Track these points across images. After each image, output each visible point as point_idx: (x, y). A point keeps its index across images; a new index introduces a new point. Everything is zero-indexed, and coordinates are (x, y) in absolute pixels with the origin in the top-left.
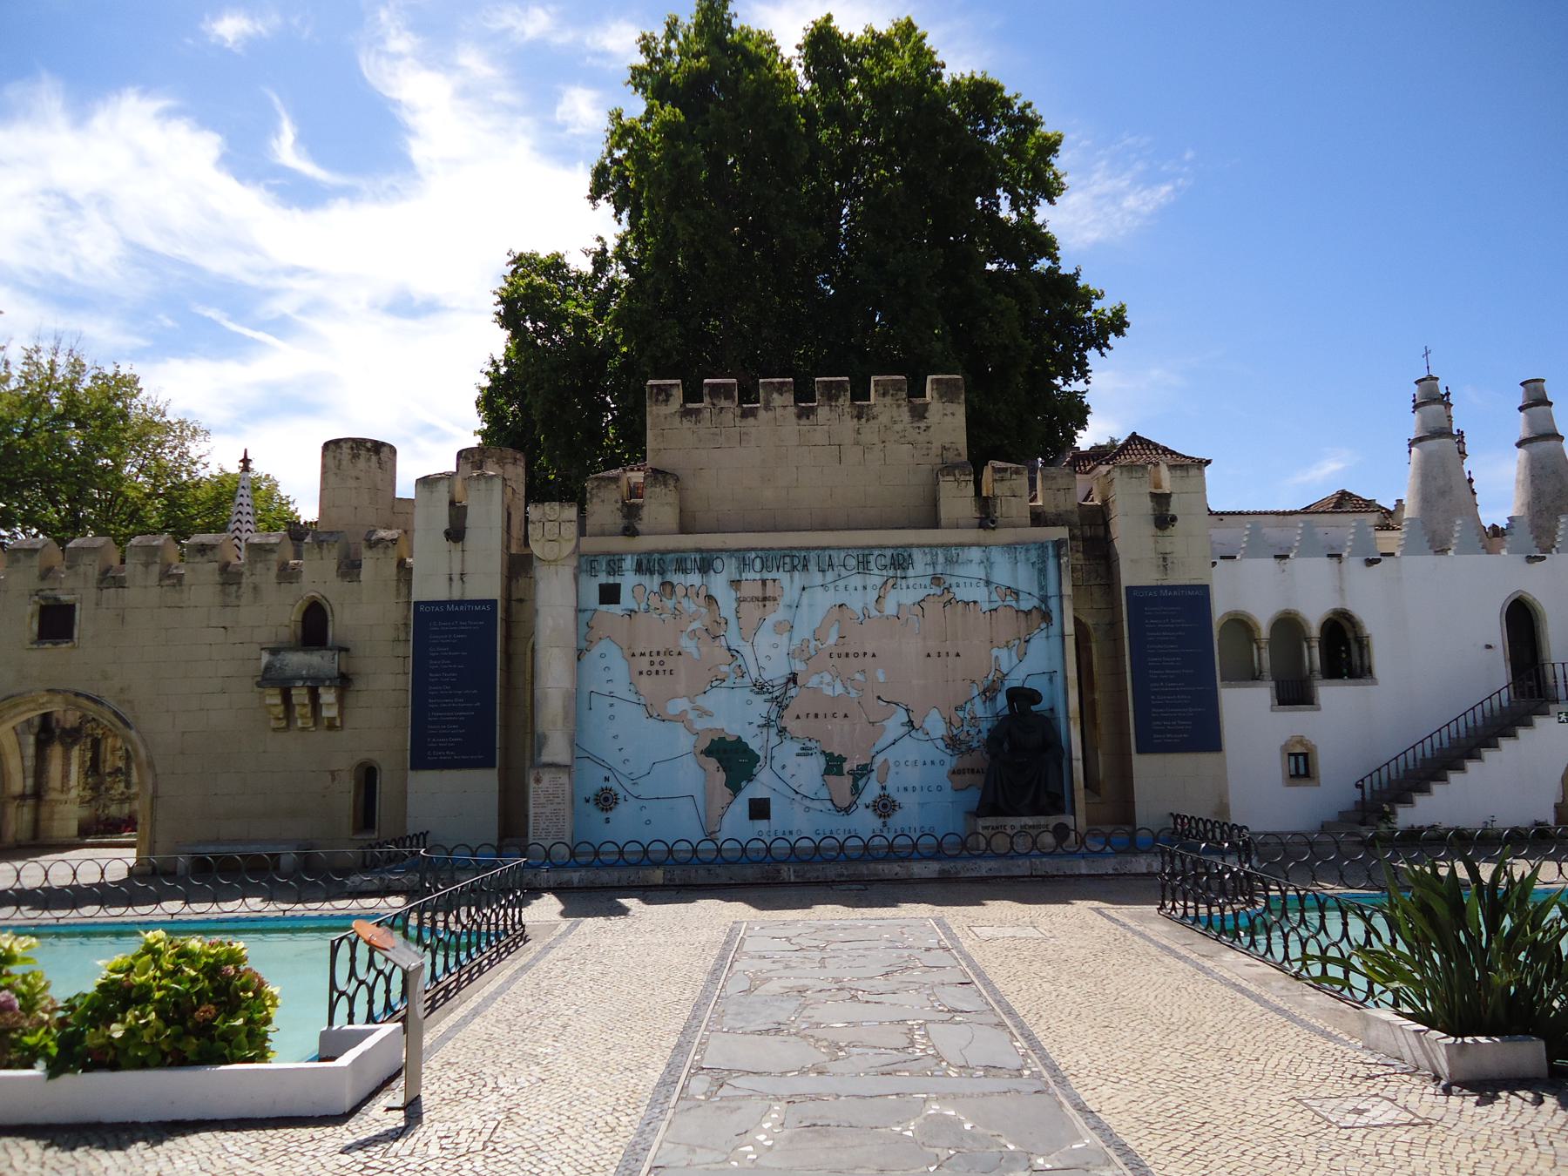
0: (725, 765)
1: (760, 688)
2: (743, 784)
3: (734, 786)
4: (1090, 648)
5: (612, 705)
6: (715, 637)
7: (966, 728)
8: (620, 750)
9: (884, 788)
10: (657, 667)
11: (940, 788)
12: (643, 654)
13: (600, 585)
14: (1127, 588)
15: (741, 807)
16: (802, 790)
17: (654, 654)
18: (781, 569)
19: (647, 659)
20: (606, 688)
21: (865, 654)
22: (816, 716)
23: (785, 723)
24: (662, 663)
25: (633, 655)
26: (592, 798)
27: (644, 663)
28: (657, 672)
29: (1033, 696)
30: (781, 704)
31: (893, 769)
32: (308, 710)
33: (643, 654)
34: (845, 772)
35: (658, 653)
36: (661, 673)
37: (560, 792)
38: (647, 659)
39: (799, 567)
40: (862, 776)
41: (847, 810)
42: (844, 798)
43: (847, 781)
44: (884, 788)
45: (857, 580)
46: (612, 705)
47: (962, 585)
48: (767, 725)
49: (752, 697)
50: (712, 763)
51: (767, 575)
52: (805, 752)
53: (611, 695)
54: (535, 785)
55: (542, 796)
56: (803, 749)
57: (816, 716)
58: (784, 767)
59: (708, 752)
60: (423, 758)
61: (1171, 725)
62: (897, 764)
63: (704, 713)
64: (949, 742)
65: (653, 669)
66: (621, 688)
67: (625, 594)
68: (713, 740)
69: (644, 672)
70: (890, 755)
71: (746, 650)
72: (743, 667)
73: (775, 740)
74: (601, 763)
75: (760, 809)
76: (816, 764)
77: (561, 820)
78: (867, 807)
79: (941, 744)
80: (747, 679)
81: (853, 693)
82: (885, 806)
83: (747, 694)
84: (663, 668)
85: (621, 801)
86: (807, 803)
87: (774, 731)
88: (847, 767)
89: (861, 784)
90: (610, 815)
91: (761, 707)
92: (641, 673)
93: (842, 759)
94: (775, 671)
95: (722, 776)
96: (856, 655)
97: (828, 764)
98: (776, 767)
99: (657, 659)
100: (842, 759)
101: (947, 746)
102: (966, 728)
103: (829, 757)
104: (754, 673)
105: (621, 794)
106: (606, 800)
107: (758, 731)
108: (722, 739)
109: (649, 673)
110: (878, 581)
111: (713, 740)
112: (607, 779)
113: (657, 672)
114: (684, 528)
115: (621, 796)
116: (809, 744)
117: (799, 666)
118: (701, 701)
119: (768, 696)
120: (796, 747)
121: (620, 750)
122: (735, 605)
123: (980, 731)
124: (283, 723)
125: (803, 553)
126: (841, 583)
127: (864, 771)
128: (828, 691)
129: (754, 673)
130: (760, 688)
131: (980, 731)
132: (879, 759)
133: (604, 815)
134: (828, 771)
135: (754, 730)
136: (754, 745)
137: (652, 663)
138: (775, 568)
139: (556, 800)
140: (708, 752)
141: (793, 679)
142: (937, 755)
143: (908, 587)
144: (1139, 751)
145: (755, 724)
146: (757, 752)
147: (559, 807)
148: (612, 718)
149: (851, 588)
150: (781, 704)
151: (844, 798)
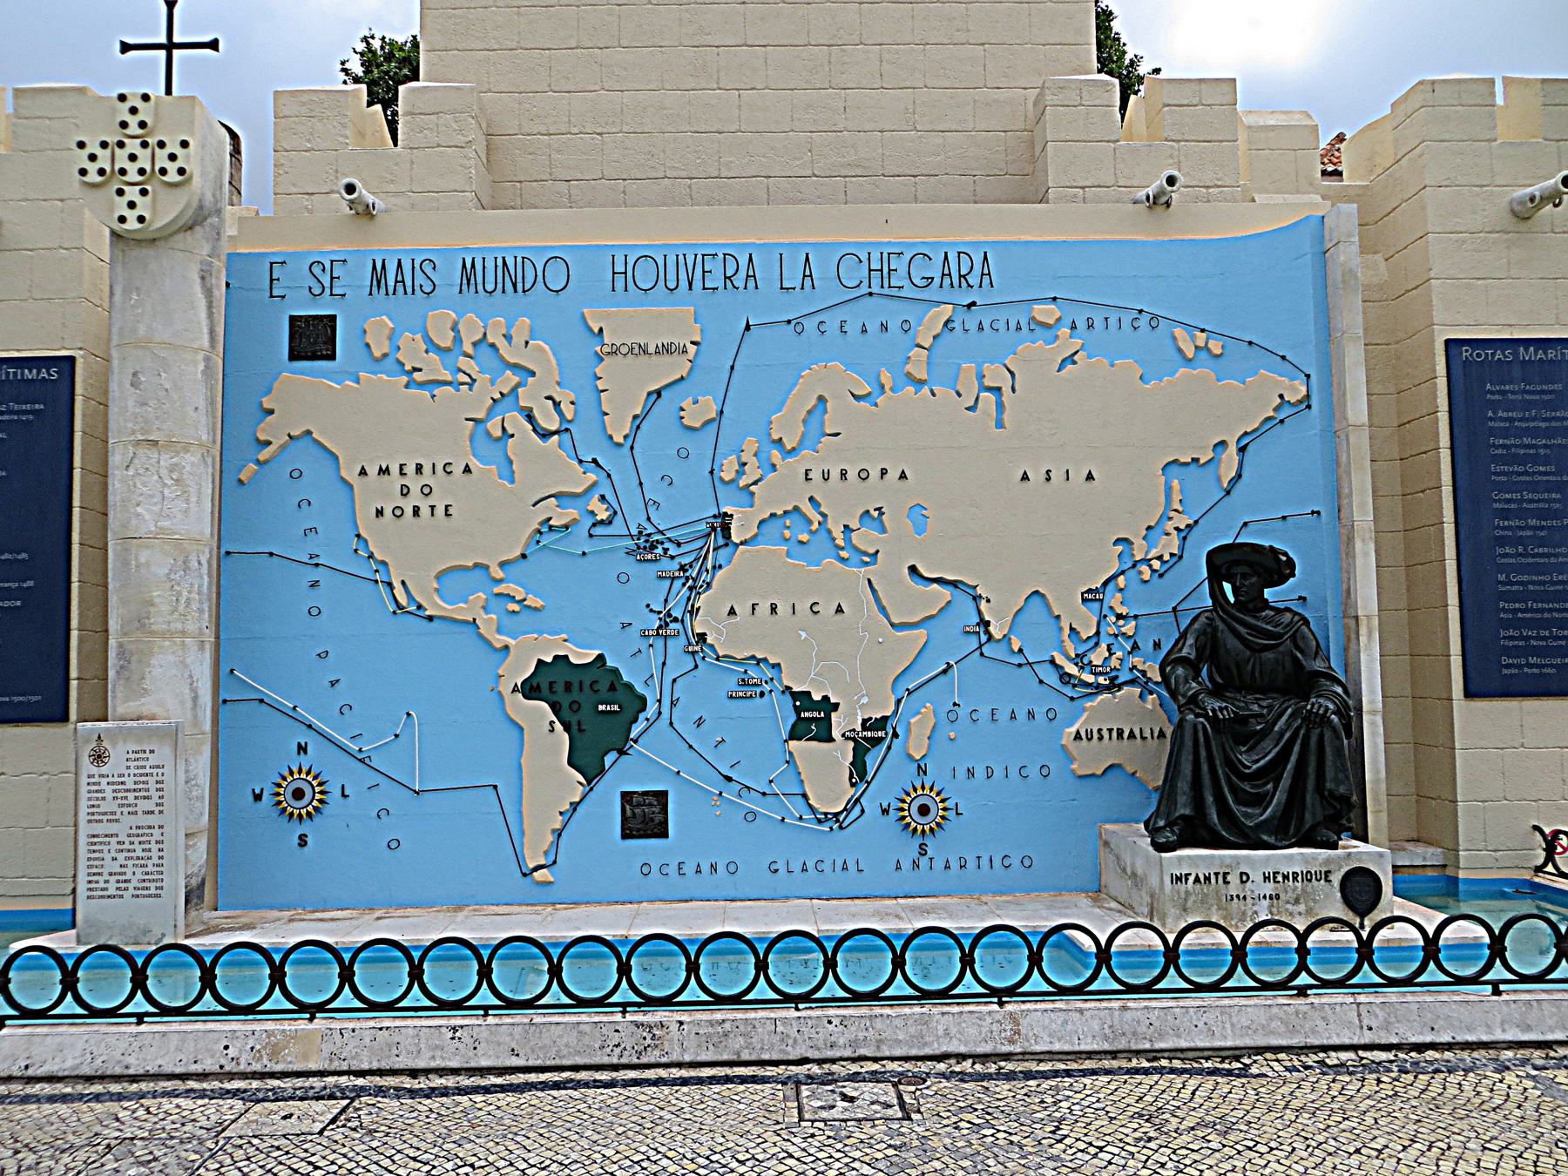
1: (647, 546)
2: (609, 759)
3: (588, 765)
5: (314, 584)
6: (545, 435)
8: (333, 684)
10: (415, 498)
12: (384, 471)
17: (410, 469)
18: (697, 284)
19: (395, 481)
21: (884, 472)
24: (427, 491)
25: (363, 472)
28: (416, 511)
29: (1276, 567)
33: (384, 471)
34: (836, 734)
35: (419, 468)
36: (425, 511)
37: (152, 786)
39: (739, 281)
46: (314, 584)
47: (1099, 323)
48: (662, 632)
49: (630, 566)
52: (748, 689)
54: (94, 770)
55: (109, 794)
56: (744, 683)
58: (700, 722)
59: (530, 689)
61: (1538, 638)
68: (540, 662)
69: (388, 512)
72: (610, 497)
73: (679, 663)
77: (155, 854)
78: (885, 812)
79: (1052, 678)
80: (618, 527)
84: (431, 501)
88: (838, 727)
89: (872, 761)
92: (380, 513)
97: (799, 718)
100: (828, 706)
107: (643, 645)
111: (540, 662)
112: (302, 749)
113: (416, 511)
121: (333, 684)
123: (1135, 647)
127: (873, 735)
129: (636, 520)
130: (647, 546)
131: (1135, 647)
137: (405, 492)
138: (684, 283)
139: (144, 805)
140: (530, 689)
143: (981, 328)
145: (638, 626)
146: (640, 688)
147: (150, 820)
148: (314, 613)
149: (853, 328)
151: (833, 793)
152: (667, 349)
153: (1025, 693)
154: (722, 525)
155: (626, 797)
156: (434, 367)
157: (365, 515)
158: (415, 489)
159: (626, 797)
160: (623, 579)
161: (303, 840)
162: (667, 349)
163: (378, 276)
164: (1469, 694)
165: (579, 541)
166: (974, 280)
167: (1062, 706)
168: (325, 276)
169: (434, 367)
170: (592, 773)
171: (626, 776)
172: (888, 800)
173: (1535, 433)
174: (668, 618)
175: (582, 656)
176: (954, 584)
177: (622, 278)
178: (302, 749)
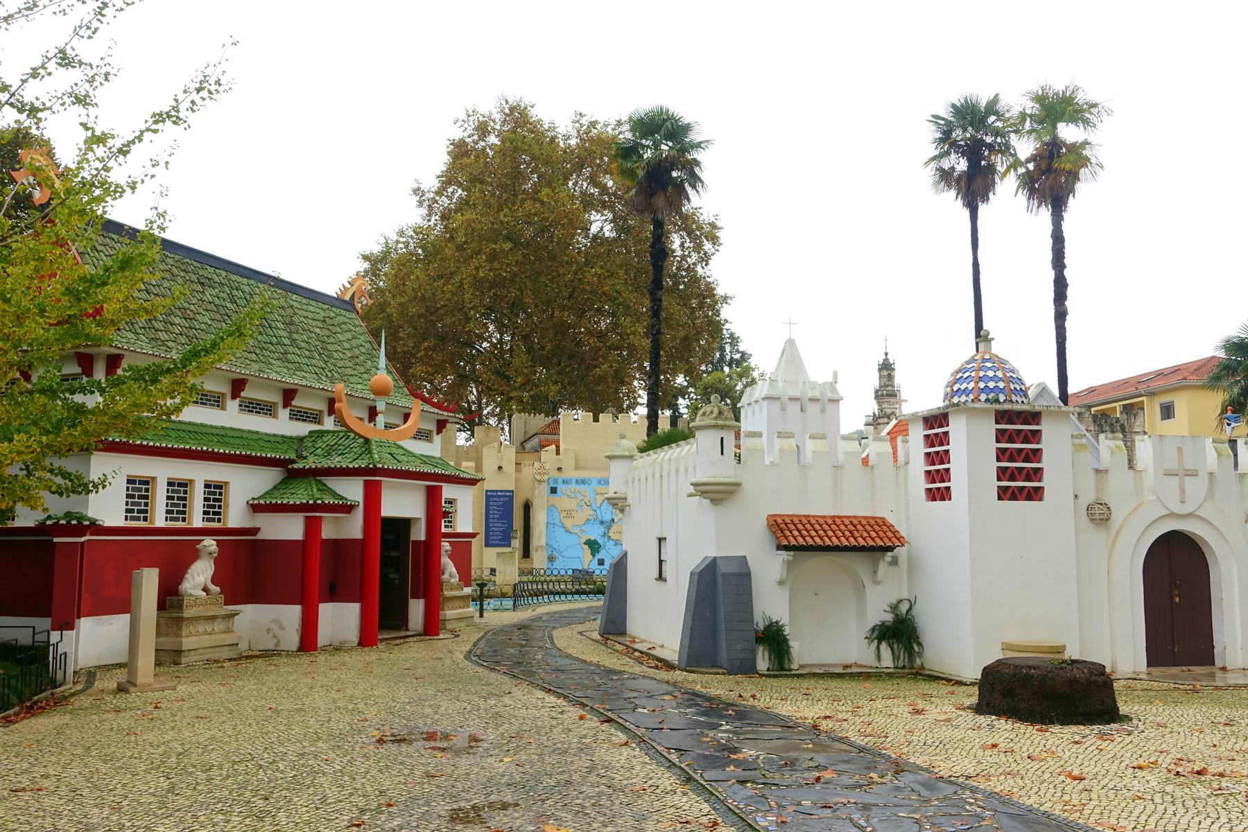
0: (591, 547)
1: (602, 523)
3: (593, 554)
15: (595, 561)
20: (552, 522)
27: (564, 514)
50: (587, 546)
53: (554, 524)
59: (585, 543)
73: (606, 540)
91: (602, 529)
104: (600, 517)
114: (577, 468)
130: (602, 523)
140: (585, 543)
154: (613, 520)
155: (599, 560)
156: (572, 495)
157: (562, 517)
159: (599, 560)
163: (564, 481)
165: (592, 521)
168: (556, 481)
169: (572, 495)
171: (599, 556)
175: (592, 539)
177: (599, 482)
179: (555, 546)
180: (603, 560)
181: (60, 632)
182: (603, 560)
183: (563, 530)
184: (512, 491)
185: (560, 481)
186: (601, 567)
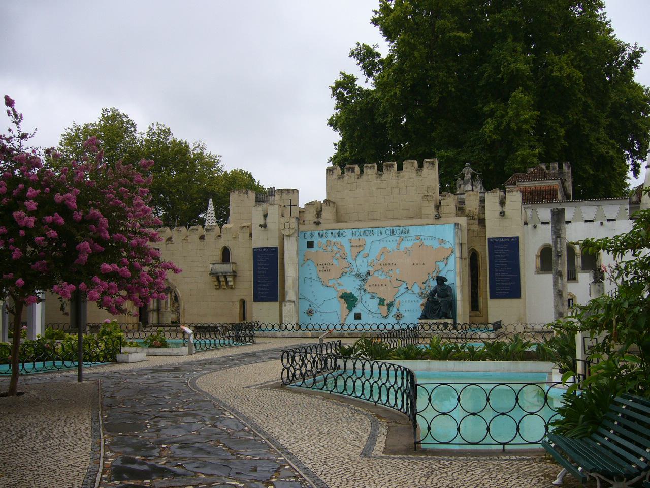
1: (358, 276)
2: (353, 308)
3: (350, 308)
4: (479, 260)
5: (311, 282)
7: (426, 290)
9: (398, 310)
10: (325, 269)
11: (417, 310)
12: (321, 265)
13: (308, 242)
14: (488, 238)
15: (352, 315)
16: (371, 310)
19: (322, 266)
20: (310, 276)
22: (376, 285)
23: (365, 288)
24: (327, 268)
26: (306, 311)
27: (321, 268)
30: (364, 281)
31: (402, 304)
32: (224, 283)
33: (321, 265)
38: (322, 266)
40: (391, 306)
41: (386, 317)
42: (385, 314)
43: (386, 307)
44: (398, 310)
45: (391, 238)
50: (343, 300)
51: (360, 238)
52: (373, 297)
57: (376, 285)
59: (341, 297)
60: (257, 299)
62: (403, 302)
63: (340, 284)
64: (421, 294)
65: (324, 270)
66: (314, 276)
67: (315, 245)
70: (401, 299)
71: (353, 263)
73: (363, 293)
74: (309, 301)
75: (358, 316)
76: (377, 301)
79: (418, 296)
81: (389, 279)
82: (398, 316)
83: (353, 278)
85: (315, 312)
86: (374, 315)
87: (362, 291)
88: (386, 303)
89: (391, 308)
90: (311, 317)
91: (358, 282)
93: (384, 300)
94: (363, 271)
95: (346, 305)
96: (389, 264)
98: (363, 303)
99: (325, 266)
100: (384, 300)
101: (420, 296)
102: (426, 290)
103: (380, 299)
104: (356, 270)
105: (315, 310)
106: (310, 313)
108: (346, 293)
109: (323, 271)
110: (398, 239)
112: (310, 306)
115: (314, 311)
116: (374, 295)
117: (370, 269)
118: (340, 281)
119: (360, 279)
120: (370, 296)
122: (350, 248)
124: (218, 287)
125: (371, 229)
126: (385, 240)
127: (391, 304)
128: (380, 277)
130: (358, 276)
132: (397, 300)
133: (310, 317)
134: (380, 304)
135: (356, 290)
136: (356, 295)
140: (341, 297)
141: (368, 273)
142: (416, 299)
144: (491, 298)
146: (357, 298)
149: (388, 241)
150: (364, 281)
152: (360, 245)
153: (414, 298)
158: (325, 268)
159: (355, 313)
160: (354, 281)
161: (310, 319)
162: (360, 245)
164: (491, 298)
166: (406, 233)
167: (419, 300)
170: (350, 310)
171: (356, 310)
172: (393, 314)
173: (503, 254)
174: (361, 287)
175: (349, 292)
176: (403, 281)
178: (310, 306)
179: (313, 301)
180: (360, 314)
181: (32, 363)
182: (360, 314)
183: (320, 284)
184: (276, 248)
185: (316, 234)
186: (358, 321)
